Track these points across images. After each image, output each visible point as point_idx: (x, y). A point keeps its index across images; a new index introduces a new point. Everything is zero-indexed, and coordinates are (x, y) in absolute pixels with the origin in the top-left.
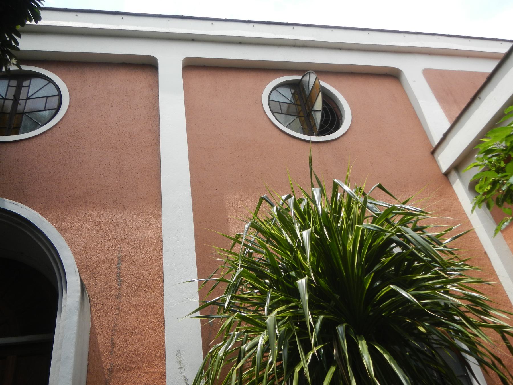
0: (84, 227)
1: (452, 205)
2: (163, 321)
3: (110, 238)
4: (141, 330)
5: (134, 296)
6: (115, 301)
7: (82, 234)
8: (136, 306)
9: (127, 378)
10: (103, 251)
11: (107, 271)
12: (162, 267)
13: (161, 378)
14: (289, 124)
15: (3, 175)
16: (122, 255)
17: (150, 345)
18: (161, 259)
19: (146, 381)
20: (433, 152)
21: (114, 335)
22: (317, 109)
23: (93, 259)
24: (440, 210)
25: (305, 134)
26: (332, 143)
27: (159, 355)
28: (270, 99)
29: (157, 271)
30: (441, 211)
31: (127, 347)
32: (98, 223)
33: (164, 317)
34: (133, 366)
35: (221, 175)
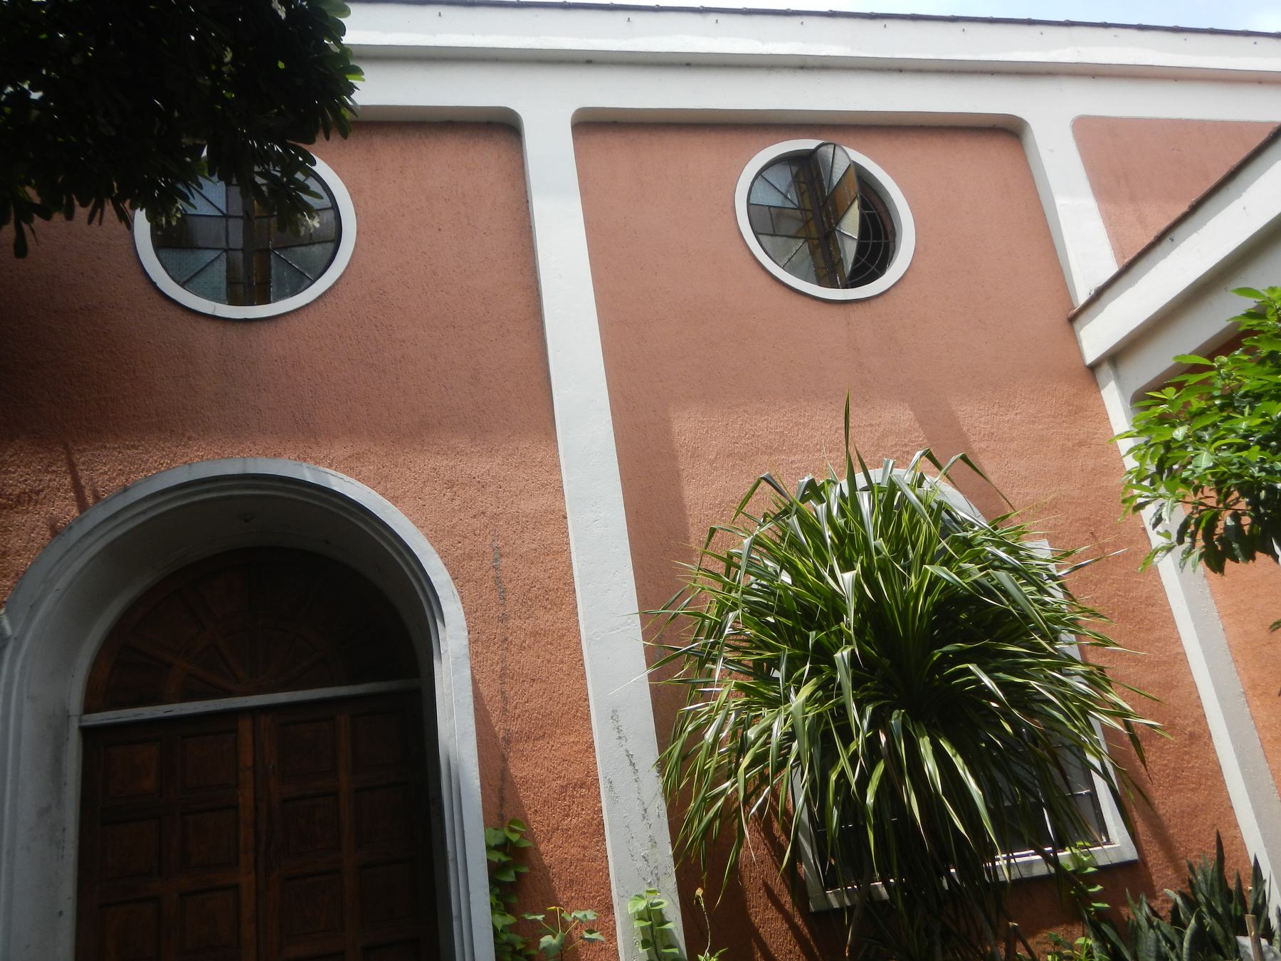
0: (427, 493)
1: (1096, 434)
2: (580, 660)
3: (474, 512)
4: (545, 674)
5: (529, 617)
6: (498, 626)
7: (424, 506)
8: (535, 634)
9: (534, 751)
10: (466, 538)
11: (478, 574)
12: (570, 566)
13: (586, 751)
14: (789, 259)
15: (265, 390)
16: (500, 543)
17: (564, 699)
18: (566, 550)
19: (563, 756)
20: (1072, 319)
21: (504, 683)
22: (847, 231)
23: (451, 552)
24: (1070, 444)
25: (820, 282)
26: (873, 303)
27: (579, 714)
28: (751, 202)
29: (562, 573)
30: (1074, 446)
31: (527, 702)
32: (450, 484)
33: (582, 653)
34: (541, 733)
35: (661, 381)
